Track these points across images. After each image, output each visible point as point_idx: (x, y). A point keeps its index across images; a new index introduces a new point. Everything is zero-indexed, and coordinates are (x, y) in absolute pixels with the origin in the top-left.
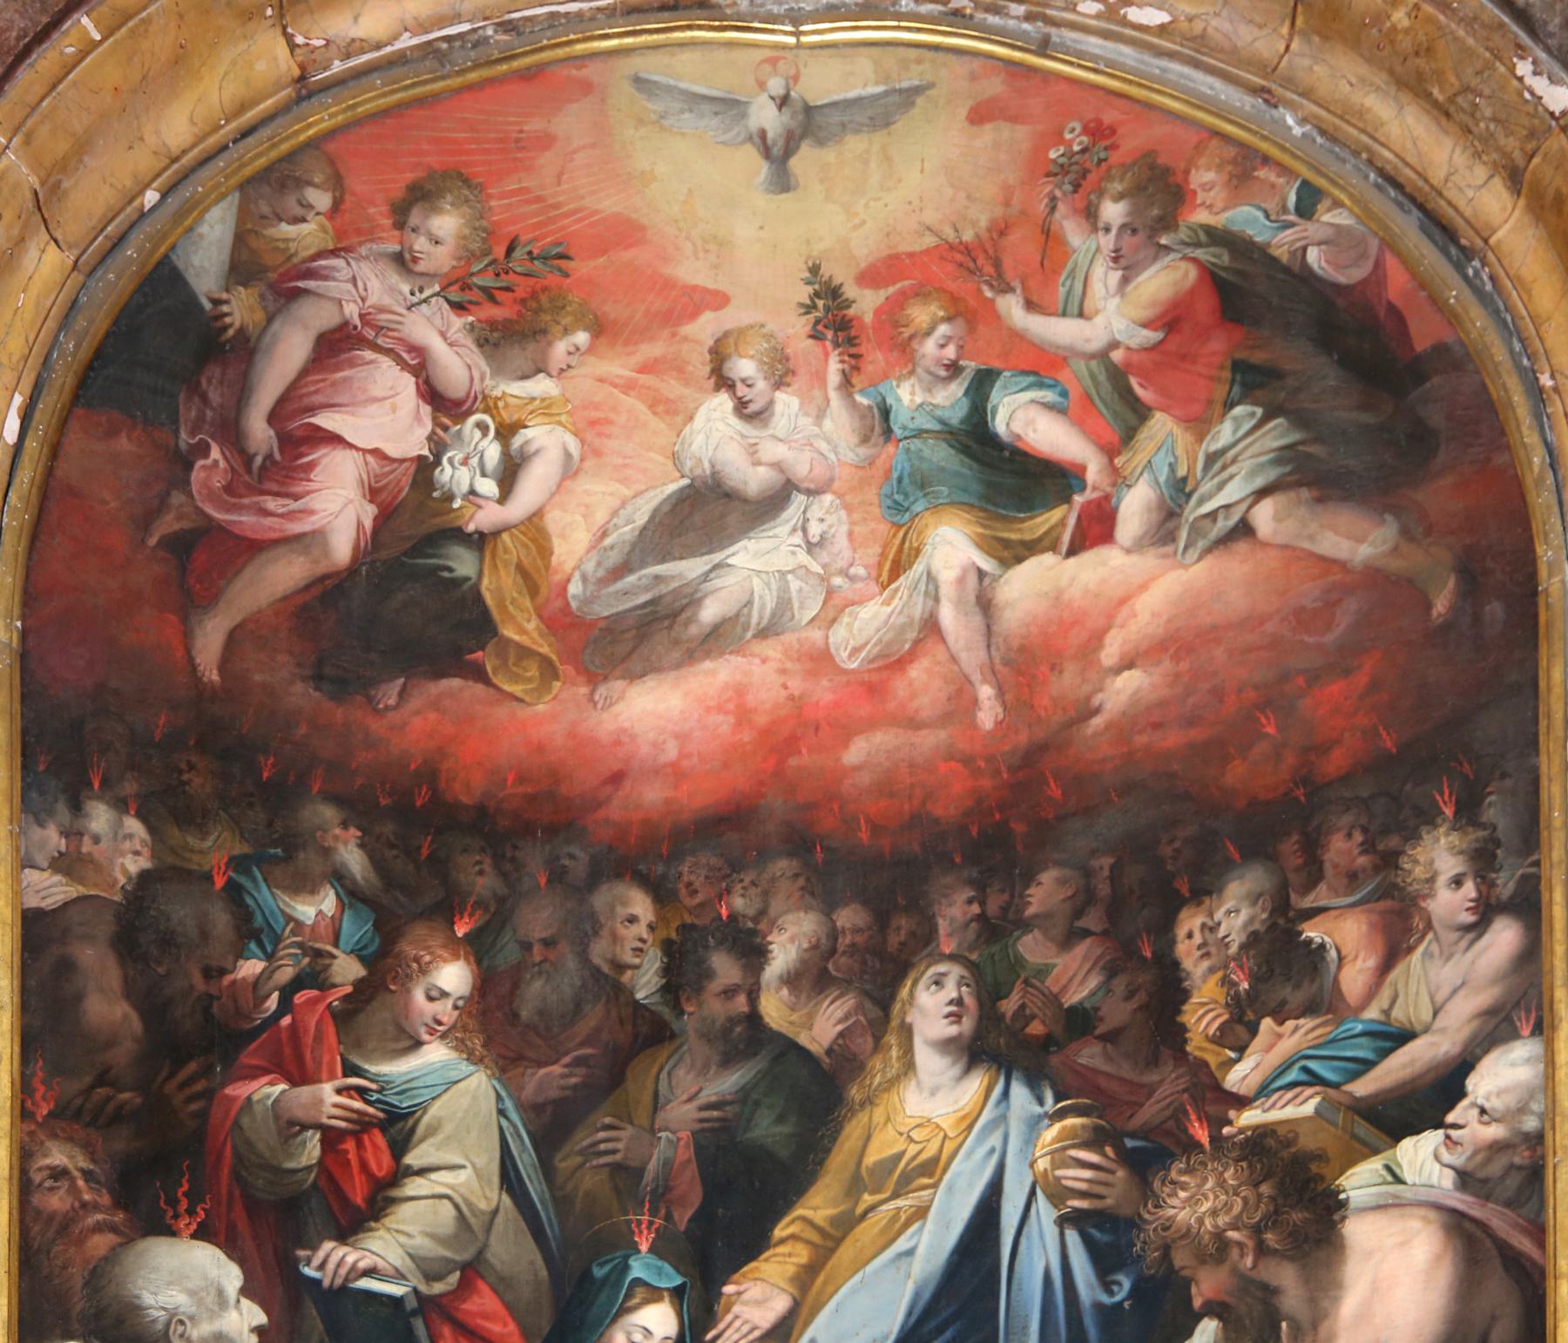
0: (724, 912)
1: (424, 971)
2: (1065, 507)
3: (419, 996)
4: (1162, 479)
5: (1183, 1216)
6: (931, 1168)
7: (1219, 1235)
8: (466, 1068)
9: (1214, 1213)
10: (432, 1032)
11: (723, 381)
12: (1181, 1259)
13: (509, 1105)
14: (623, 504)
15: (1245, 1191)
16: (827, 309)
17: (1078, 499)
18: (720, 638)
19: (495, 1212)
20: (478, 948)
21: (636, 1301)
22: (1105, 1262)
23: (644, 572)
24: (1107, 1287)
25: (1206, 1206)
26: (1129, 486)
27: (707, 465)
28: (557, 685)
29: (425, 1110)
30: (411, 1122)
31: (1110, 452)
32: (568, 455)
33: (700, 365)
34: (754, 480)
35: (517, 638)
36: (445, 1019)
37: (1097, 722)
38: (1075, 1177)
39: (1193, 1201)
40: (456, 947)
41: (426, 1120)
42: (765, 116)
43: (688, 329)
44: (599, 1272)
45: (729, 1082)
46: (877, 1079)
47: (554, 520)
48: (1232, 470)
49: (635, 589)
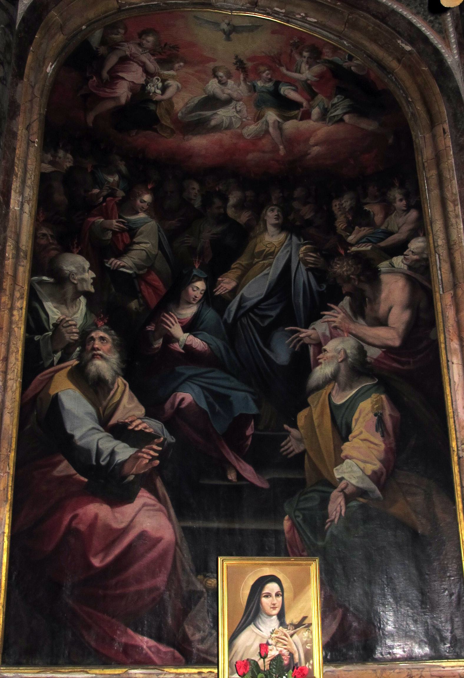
0: (217, 189)
1: (140, 196)
2: (298, 111)
3: (138, 202)
4: (321, 108)
6: (273, 254)
7: (348, 276)
8: (150, 219)
9: (347, 271)
10: (141, 210)
11: (215, 76)
12: (339, 281)
13: (161, 229)
14: (191, 99)
15: (354, 266)
16: (240, 65)
17: (302, 109)
18: (217, 128)
19: (157, 255)
20: (154, 192)
21: (195, 280)
22: (320, 280)
23: (197, 113)
24: (320, 287)
25: (344, 269)
26: (314, 108)
27: (212, 92)
28: (175, 135)
29: (139, 229)
30: (135, 231)
31: (308, 101)
32: (178, 87)
33: (210, 72)
34: (224, 96)
35: (165, 124)
36: (145, 208)
37: (310, 156)
39: (341, 267)
40: (148, 191)
41: (139, 230)
42: (224, 26)
43: (207, 65)
44: (185, 272)
45: (219, 229)
46: (257, 232)
47: (175, 100)
48: (338, 108)
49: (194, 116)
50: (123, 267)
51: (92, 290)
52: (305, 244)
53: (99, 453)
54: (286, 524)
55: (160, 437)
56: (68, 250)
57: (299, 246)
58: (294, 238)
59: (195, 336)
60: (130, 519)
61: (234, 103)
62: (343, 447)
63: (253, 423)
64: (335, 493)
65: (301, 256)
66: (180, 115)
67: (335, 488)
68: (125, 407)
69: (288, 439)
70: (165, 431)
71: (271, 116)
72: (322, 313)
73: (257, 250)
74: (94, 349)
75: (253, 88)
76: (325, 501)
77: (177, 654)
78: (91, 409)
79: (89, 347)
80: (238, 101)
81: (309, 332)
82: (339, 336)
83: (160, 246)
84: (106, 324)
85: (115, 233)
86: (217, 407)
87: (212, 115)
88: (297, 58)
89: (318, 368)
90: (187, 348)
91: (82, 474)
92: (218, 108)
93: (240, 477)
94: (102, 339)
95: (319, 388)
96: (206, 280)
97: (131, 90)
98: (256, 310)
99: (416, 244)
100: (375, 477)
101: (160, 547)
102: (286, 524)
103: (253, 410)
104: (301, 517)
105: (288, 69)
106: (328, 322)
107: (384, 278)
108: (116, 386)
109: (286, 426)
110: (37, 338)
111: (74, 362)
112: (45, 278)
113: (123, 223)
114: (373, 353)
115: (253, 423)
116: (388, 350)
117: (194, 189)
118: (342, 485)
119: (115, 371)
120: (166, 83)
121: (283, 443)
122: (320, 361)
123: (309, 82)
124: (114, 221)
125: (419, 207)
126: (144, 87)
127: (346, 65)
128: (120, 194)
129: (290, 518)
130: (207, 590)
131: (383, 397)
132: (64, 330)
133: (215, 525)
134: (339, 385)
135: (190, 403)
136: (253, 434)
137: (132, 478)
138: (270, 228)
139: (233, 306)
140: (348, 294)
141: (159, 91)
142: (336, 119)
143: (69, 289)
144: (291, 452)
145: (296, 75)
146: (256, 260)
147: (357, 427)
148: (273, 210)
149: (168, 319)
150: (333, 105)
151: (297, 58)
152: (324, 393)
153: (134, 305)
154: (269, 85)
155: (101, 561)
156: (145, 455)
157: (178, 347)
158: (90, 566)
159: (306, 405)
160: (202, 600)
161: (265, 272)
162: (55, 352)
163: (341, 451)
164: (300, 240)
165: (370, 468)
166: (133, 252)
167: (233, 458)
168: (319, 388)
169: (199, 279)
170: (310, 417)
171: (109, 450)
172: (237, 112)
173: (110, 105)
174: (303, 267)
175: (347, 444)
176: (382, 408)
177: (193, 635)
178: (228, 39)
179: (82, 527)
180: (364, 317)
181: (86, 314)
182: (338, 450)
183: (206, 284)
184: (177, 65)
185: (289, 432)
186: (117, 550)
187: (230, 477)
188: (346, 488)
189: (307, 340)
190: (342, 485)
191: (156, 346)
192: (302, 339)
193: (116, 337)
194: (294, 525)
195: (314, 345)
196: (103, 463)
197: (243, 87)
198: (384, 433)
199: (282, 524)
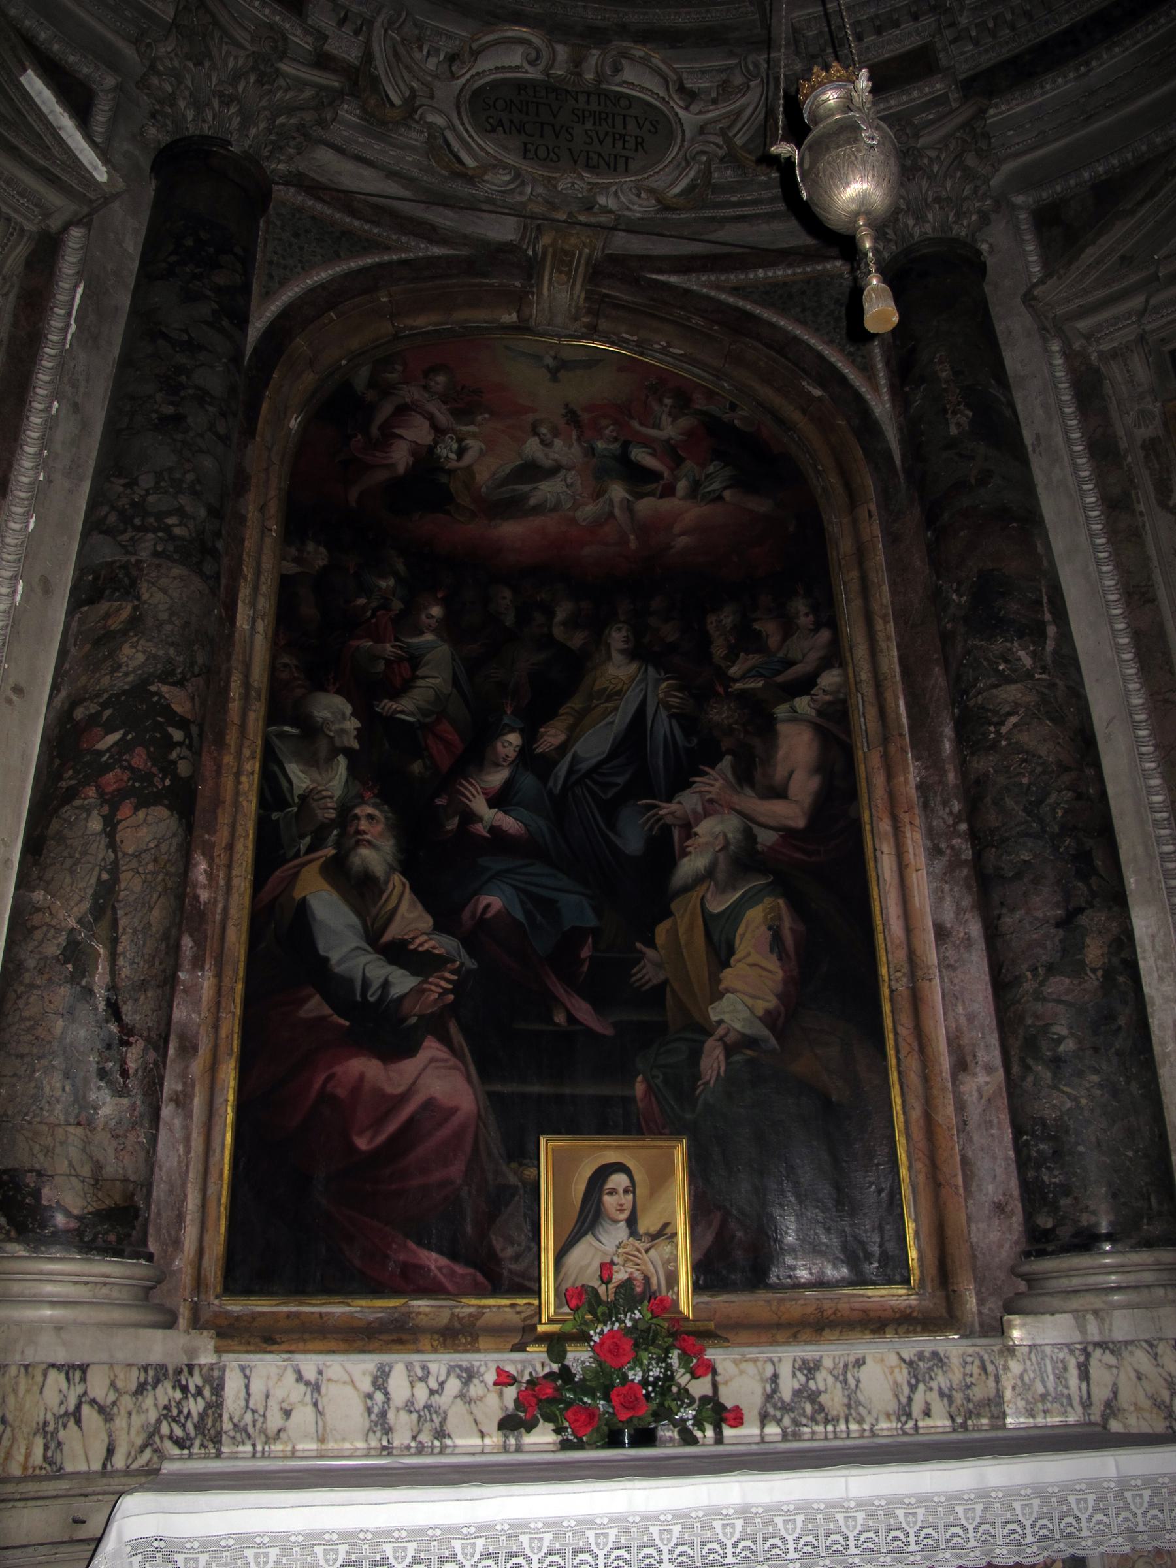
3: (423, 617)
5: (716, 718)
6: (619, 693)
9: (727, 718)
11: (536, 434)
17: (662, 482)
18: (538, 510)
31: (672, 470)
32: (481, 450)
34: (548, 464)
38: (673, 701)
42: (549, 361)
50: (402, 712)
51: (356, 746)
52: (667, 679)
53: (366, 983)
54: (640, 1088)
55: (454, 961)
56: (323, 688)
57: (658, 682)
58: (651, 670)
59: (506, 812)
60: (410, 1081)
61: (563, 472)
62: (722, 976)
63: (590, 940)
64: (710, 1043)
65: (661, 696)
66: (484, 490)
67: (711, 1035)
68: (403, 917)
69: (642, 963)
70: (462, 950)
71: (618, 492)
72: (692, 779)
73: (596, 688)
74: (358, 832)
75: (591, 451)
76: (695, 1055)
77: (480, 1278)
78: (354, 919)
79: (352, 830)
80: (569, 470)
81: (673, 807)
82: (716, 812)
83: (456, 682)
84: (376, 796)
85: (389, 663)
86: (539, 918)
87: (531, 491)
88: (656, 407)
89: (686, 860)
90: (495, 830)
91: (340, 1016)
92: (541, 481)
93: (571, 1019)
94: (370, 817)
95: (687, 889)
96: (522, 731)
97: (413, 453)
98: (595, 776)
99: (829, 679)
100: (769, 1019)
101: (456, 1121)
102: (640, 1088)
103: (591, 921)
104: (661, 1077)
105: (641, 424)
106: (700, 792)
107: (782, 728)
108: (390, 886)
109: (638, 945)
110: (275, 816)
111: (330, 851)
112: (287, 728)
113: (401, 648)
114: (766, 838)
115: (590, 940)
116: (788, 834)
117: (504, 598)
118: (721, 1031)
119: (389, 864)
120: (464, 444)
121: (635, 970)
122: (689, 849)
123: (672, 442)
124: (388, 645)
125: (833, 624)
126: (431, 449)
127: (726, 417)
128: (397, 605)
129: (645, 1079)
130: (524, 1184)
131: (781, 901)
132: (314, 804)
133: (535, 1089)
134: (716, 885)
135: (499, 912)
136: (591, 957)
137: (413, 1020)
138: (617, 657)
139: (562, 769)
140: (730, 751)
141: (453, 456)
142: (712, 496)
143: (323, 746)
144: (647, 982)
145: (654, 432)
146: (595, 702)
147: (742, 947)
148: (619, 629)
149: (466, 788)
150: (707, 476)
151: (656, 407)
152: (694, 896)
153: (417, 767)
154: (615, 446)
155: (369, 1143)
156: (433, 988)
157: (480, 829)
158: (352, 1148)
159: (668, 914)
160: (517, 1198)
161: (609, 719)
162: (303, 836)
163: (719, 981)
164: (659, 673)
165: (761, 1006)
166: (416, 691)
167: (562, 991)
168: (687, 889)
169: (512, 730)
170: (674, 932)
171: (381, 980)
172: (568, 486)
173: (381, 475)
174: (663, 713)
175: (728, 970)
176: (779, 917)
177: (503, 1250)
178: (554, 378)
179: (341, 1093)
180: (752, 785)
181: (347, 781)
182: (715, 980)
183: (523, 737)
184: (479, 418)
185: (644, 954)
186: (392, 1126)
187: (557, 1020)
188: (726, 1035)
189: (669, 820)
190: (721, 1031)
191: (449, 828)
192: (662, 818)
193: (390, 815)
194: (650, 1089)
195: (681, 826)
196: (372, 999)
197: (576, 450)
198: (782, 956)
199: (633, 1087)
